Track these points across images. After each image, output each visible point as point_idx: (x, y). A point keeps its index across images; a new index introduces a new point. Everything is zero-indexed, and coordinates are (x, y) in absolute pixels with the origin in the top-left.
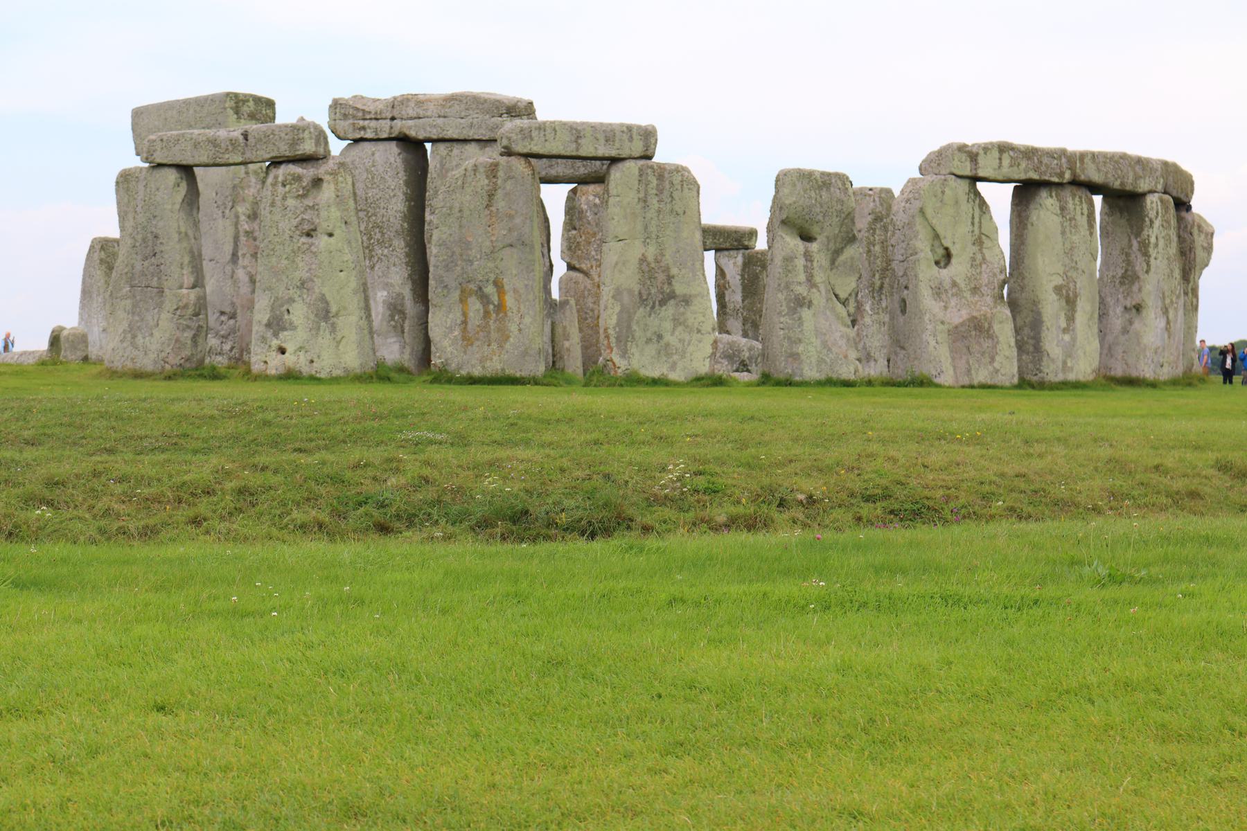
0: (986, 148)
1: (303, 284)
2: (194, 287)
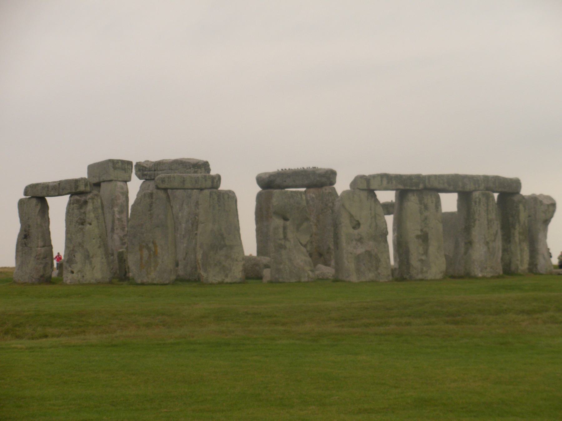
0: (374, 177)
1: (81, 245)
2: (43, 246)
